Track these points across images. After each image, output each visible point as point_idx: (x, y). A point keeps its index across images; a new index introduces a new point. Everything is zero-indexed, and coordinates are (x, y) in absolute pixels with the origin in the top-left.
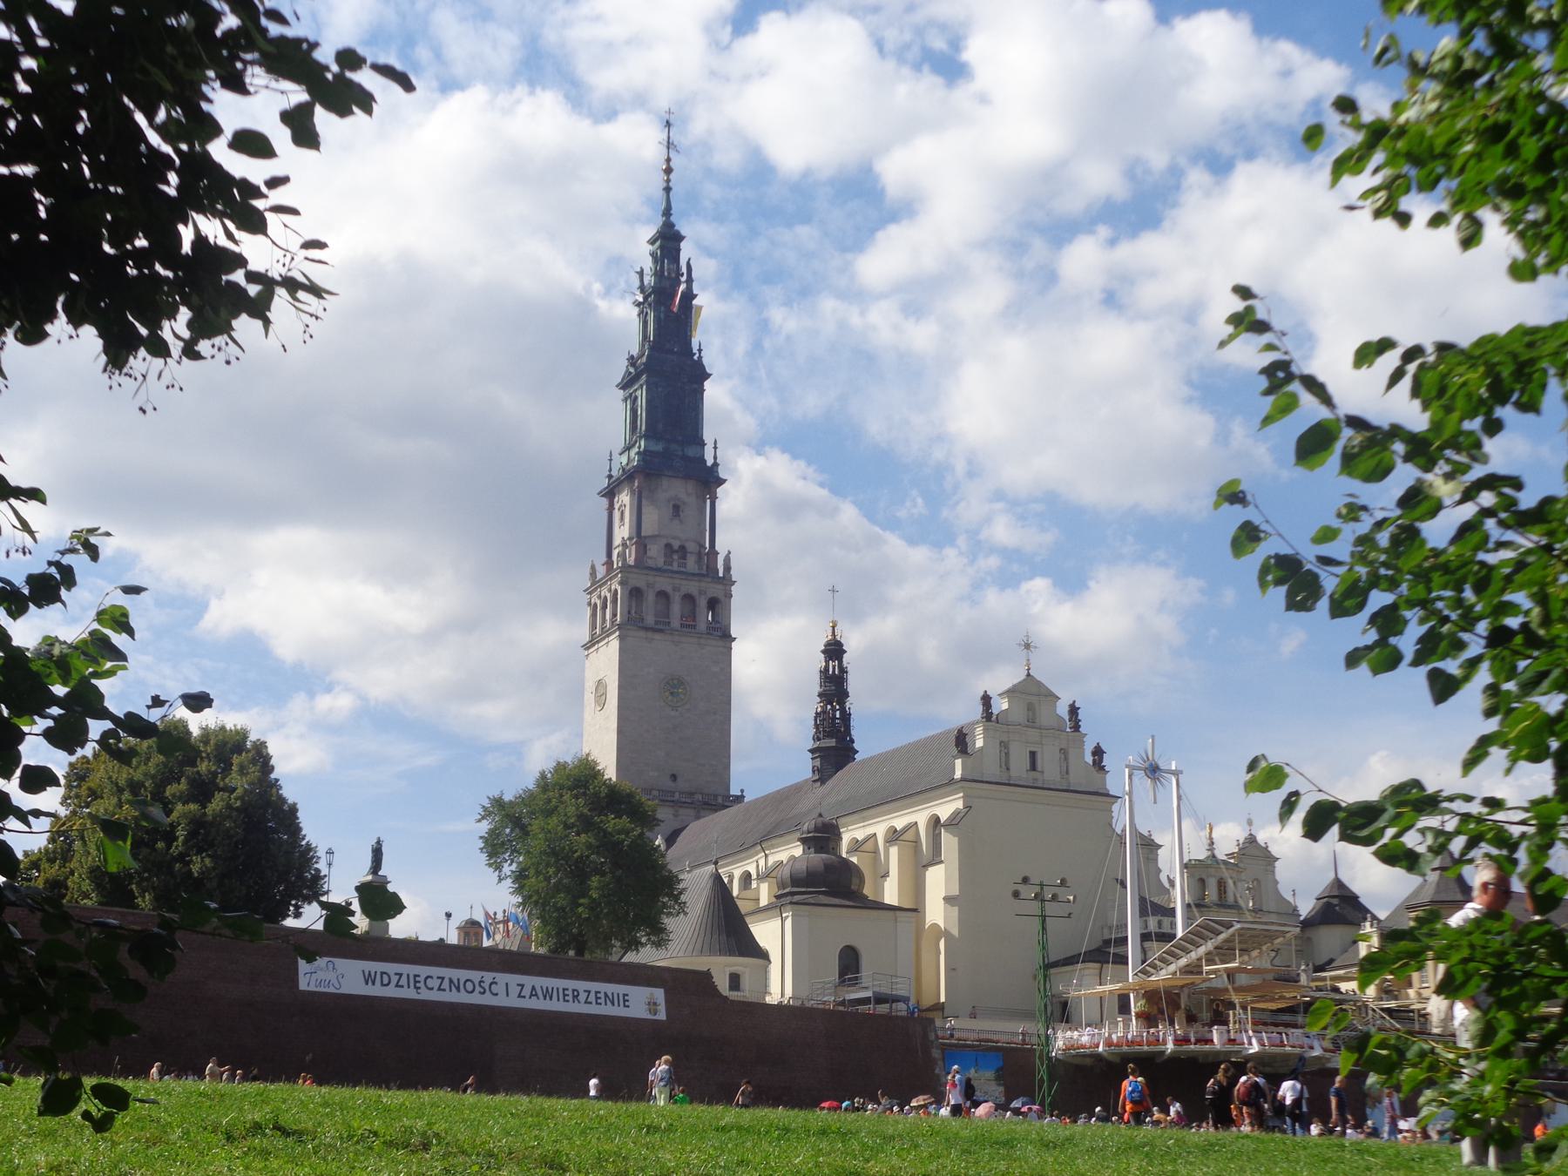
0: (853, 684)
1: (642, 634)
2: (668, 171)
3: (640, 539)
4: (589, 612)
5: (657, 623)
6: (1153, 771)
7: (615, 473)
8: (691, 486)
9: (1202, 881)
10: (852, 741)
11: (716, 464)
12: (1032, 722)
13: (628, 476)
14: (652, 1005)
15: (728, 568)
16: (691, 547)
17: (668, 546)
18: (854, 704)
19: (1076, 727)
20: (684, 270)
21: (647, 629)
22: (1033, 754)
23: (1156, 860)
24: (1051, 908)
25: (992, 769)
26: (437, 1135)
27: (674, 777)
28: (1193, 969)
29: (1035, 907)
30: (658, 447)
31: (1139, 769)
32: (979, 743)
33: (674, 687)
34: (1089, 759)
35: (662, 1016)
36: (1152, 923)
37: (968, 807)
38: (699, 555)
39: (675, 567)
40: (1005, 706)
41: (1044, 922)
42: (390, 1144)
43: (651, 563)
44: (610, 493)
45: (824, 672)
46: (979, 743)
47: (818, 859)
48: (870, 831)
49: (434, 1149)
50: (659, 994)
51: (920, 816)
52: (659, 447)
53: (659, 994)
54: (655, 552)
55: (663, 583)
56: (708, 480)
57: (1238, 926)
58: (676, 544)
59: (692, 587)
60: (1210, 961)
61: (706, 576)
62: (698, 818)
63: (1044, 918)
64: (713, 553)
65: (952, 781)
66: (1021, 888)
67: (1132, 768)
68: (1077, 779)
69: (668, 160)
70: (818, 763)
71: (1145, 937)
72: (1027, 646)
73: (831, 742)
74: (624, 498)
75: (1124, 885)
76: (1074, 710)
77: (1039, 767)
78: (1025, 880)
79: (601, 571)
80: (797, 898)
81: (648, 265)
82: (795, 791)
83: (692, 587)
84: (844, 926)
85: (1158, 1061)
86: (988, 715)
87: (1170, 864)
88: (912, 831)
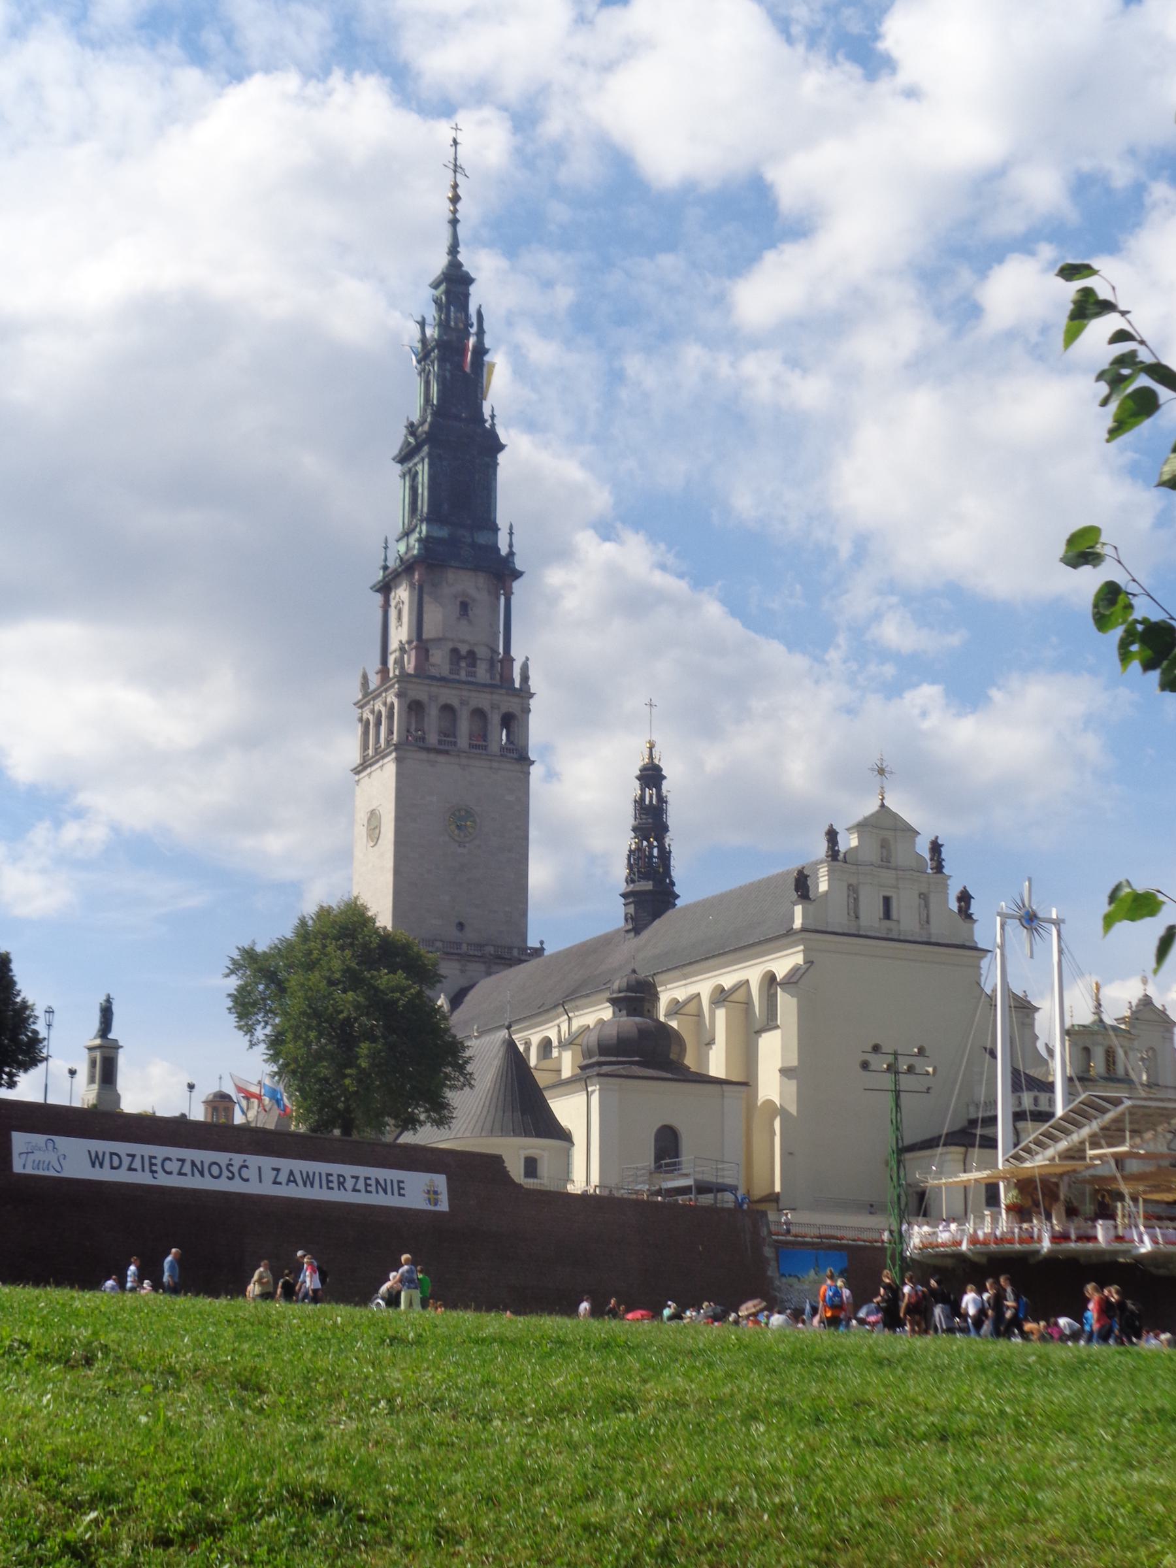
0: (674, 816)
1: (423, 755)
2: (455, 199)
3: (421, 643)
4: (359, 729)
5: (440, 742)
6: (1030, 920)
7: (392, 563)
8: (482, 579)
9: (1087, 1050)
10: (673, 884)
11: (511, 554)
12: (886, 862)
13: (407, 567)
14: (432, 1194)
15: (525, 678)
16: (482, 652)
17: (455, 651)
18: (673, 840)
19: (939, 868)
20: (474, 319)
21: (429, 750)
22: (887, 901)
23: (1032, 1025)
24: (906, 1082)
25: (838, 918)
26: (105, 1348)
27: (461, 926)
28: (1075, 1154)
29: (887, 1080)
30: (443, 533)
31: (1012, 917)
32: (823, 886)
33: (461, 819)
34: (954, 905)
35: (444, 1206)
36: (1027, 1100)
37: (809, 962)
38: (492, 663)
39: (463, 676)
40: (854, 841)
41: (897, 1098)
42: (44, 1358)
43: (433, 671)
44: (385, 588)
45: (640, 802)
46: (823, 886)
47: (631, 1023)
48: (692, 990)
49: (97, 1365)
50: (440, 1181)
51: (752, 973)
52: (443, 533)
53: (440, 1181)
54: (439, 658)
55: (449, 696)
57: (1128, 1103)
58: (464, 649)
59: (482, 700)
60: (1095, 1145)
61: (501, 687)
62: (489, 974)
63: (897, 1093)
64: (508, 660)
65: (790, 932)
66: (873, 1059)
67: (1005, 917)
68: (939, 929)
69: (455, 186)
70: (631, 909)
71: (1019, 1116)
72: (881, 771)
73: (648, 886)
74: (402, 594)
75: (993, 1054)
76: (936, 848)
77: (894, 915)
78: (876, 1049)
79: (374, 681)
80: (605, 1069)
81: (431, 313)
82: (603, 944)
83: (482, 700)
84: (660, 1102)
85: (1032, 1261)
86: (833, 854)
87: (1049, 1029)
88: (743, 990)
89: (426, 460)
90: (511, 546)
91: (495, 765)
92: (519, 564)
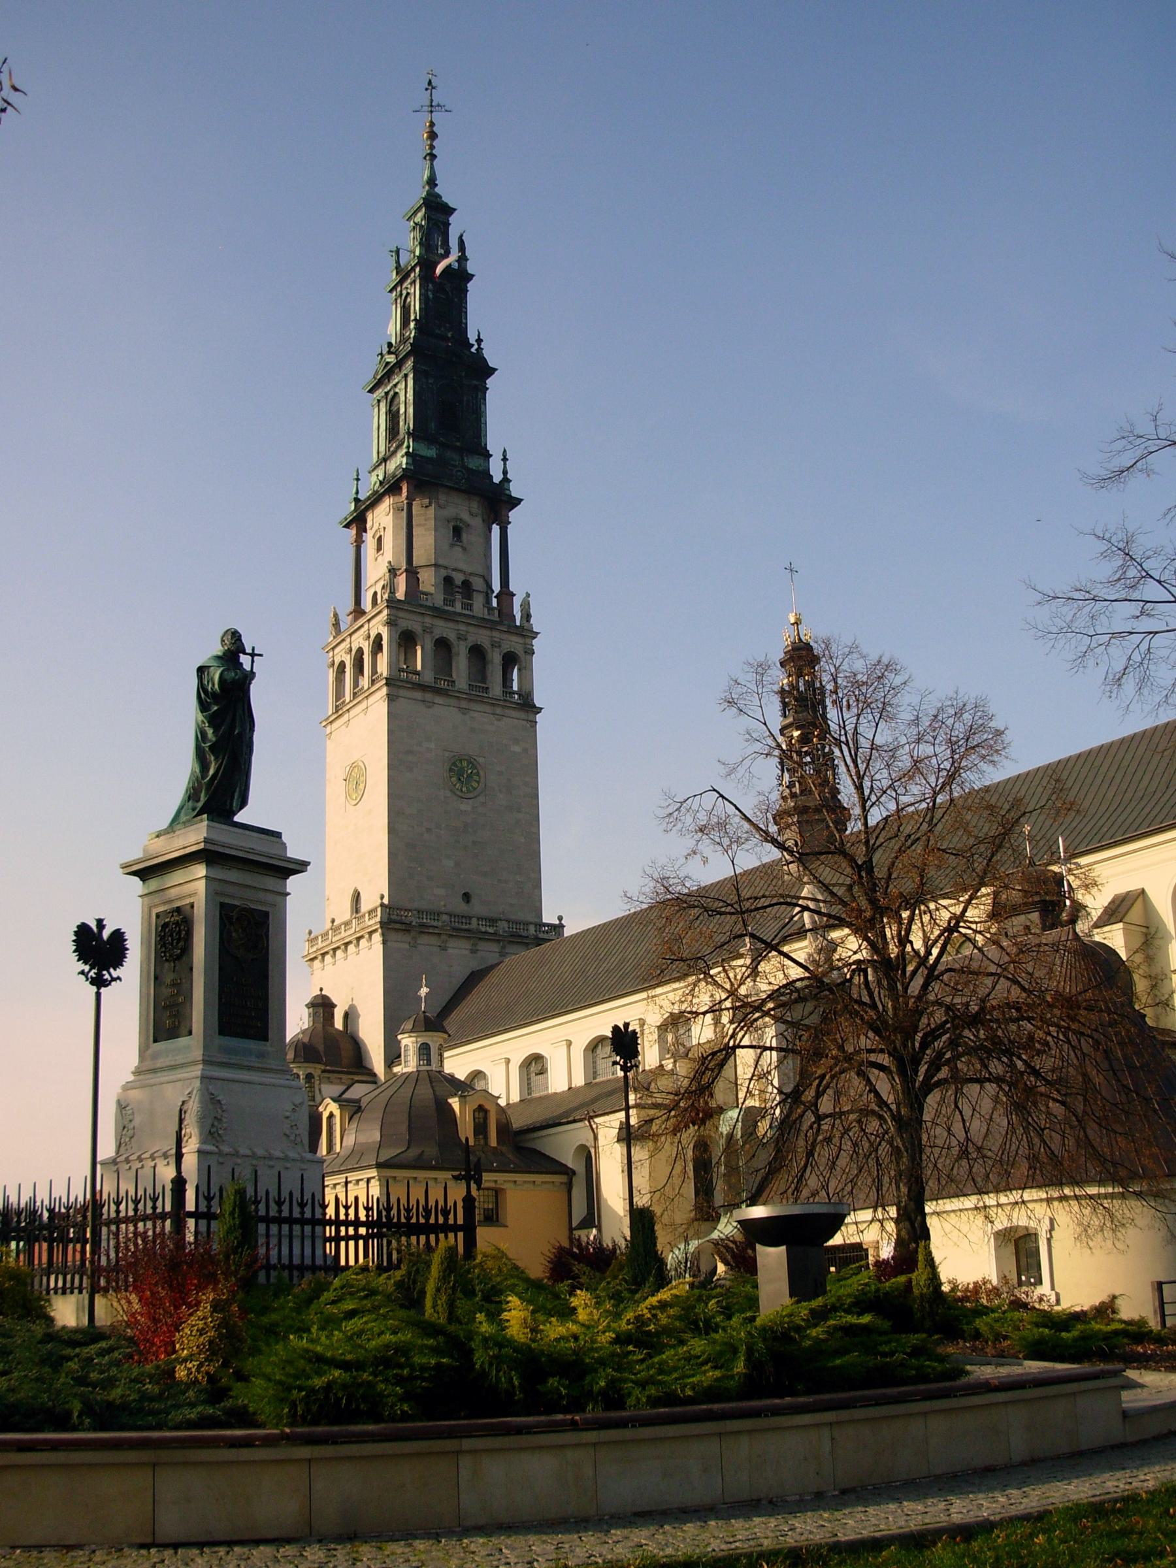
1: (418, 695)
2: (433, 136)
8: (475, 506)
11: (506, 480)
15: (527, 616)
16: (478, 584)
21: (423, 687)
27: (467, 897)
33: (463, 772)
39: (458, 607)
52: (431, 452)
55: (443, 629)
56: (498, 502)
58: (458, 578)
59: (483, 637)
61: (501, 623)
64: (506, 594)
69: (432, 124)
74: (383, 518)
83: (483, 637)
89: (411, 376)
90: (505, 472)
91: (498, 711)
92: (515, 491)
